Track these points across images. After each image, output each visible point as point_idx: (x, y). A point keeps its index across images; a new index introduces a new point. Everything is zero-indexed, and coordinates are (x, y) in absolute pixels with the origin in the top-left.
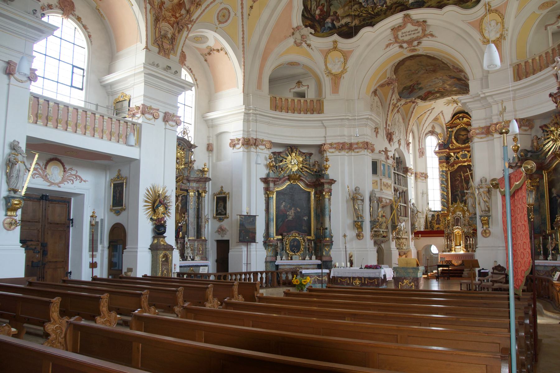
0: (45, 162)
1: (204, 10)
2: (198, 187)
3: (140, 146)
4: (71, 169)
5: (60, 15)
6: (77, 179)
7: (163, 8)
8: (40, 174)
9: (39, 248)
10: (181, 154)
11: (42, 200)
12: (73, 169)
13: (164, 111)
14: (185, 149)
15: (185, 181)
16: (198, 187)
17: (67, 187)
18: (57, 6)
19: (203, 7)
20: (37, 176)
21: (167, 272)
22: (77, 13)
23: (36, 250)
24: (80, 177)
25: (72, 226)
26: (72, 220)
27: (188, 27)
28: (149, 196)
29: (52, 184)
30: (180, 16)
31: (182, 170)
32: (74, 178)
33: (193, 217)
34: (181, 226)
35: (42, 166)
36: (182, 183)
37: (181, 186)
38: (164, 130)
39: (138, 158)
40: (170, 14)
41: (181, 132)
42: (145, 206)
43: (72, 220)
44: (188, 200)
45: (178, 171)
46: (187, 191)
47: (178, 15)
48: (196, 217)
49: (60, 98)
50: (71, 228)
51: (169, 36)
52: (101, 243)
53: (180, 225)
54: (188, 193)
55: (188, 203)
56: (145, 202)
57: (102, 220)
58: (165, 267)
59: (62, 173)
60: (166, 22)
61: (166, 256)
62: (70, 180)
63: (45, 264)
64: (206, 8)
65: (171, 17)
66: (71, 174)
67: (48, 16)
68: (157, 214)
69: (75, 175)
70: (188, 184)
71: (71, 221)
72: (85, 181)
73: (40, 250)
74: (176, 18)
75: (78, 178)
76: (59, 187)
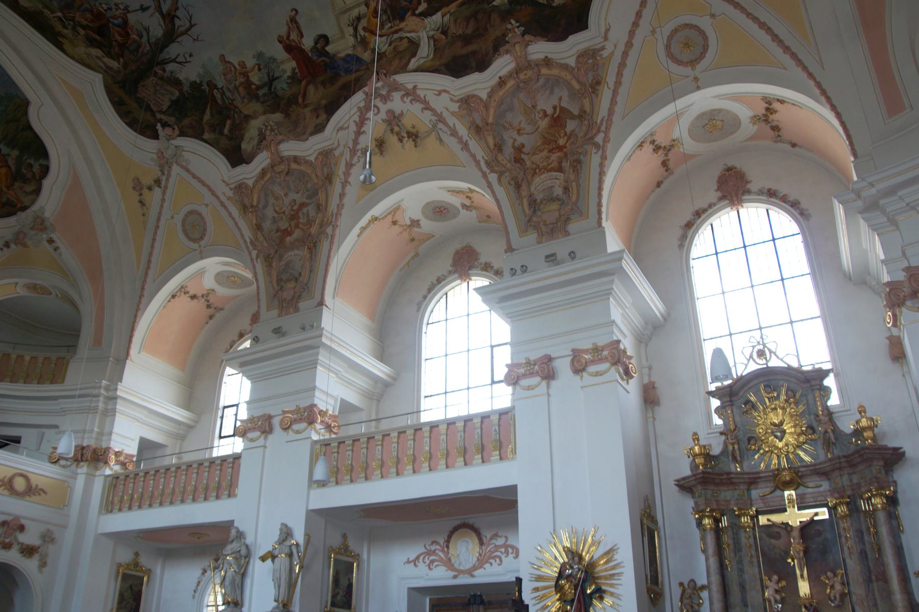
1: (618, 83)
4: (496, 536)
5: (459, 281)
7: (523, 156)
8: (441, 560)
11: (471, 606)
12: (500, 534)
18: (450, 273)
19: (611, 79)
20: (435, 564)
22: (483, 260)
24: (513, 547)
27: (597, 146)
29: (459, 572)
30: (569, 139)
32: (501, 552)
33: (861, 579)
35: (442, 544)
40: (545, 153)
41: (751, 357)
47: (561, 142)
49: (452, 414)
51: (558, 191)
60: (542, 174)
64: (620, 74)
65: (548, 158)
66: (496, 546)
67: (446, 294)
69: (501, 546)
74: (560, 148)
76: (473, 576)
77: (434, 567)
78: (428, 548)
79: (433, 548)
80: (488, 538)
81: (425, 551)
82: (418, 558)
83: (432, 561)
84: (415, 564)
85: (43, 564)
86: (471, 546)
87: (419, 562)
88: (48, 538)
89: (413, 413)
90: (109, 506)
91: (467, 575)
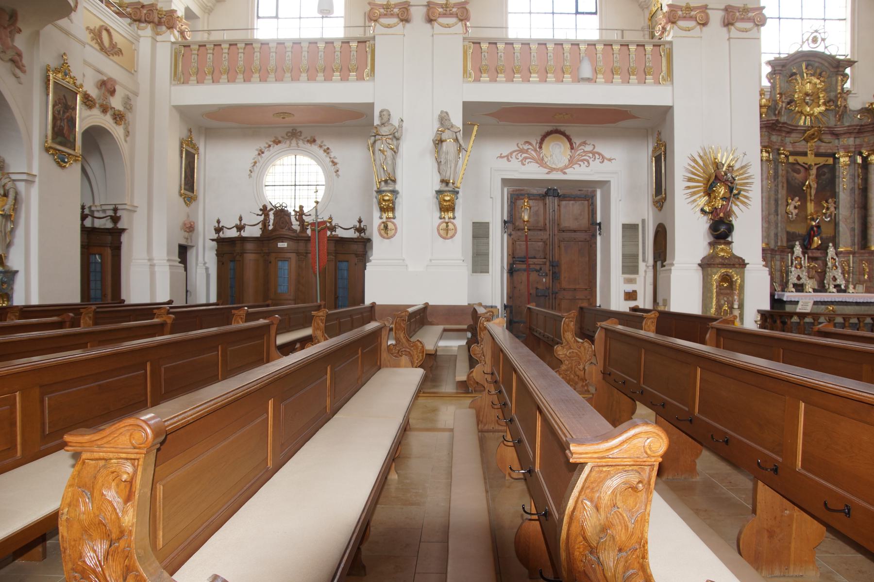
0: (539, 140)
2: (859, 145)
3: (672, 81)
4: (584, 143)
6: (595, 159)
8: (533, 158)
9: (547, 268)
10: (815, 84)
11: (547, 197)
12: (588, 142)
13: (723, 7)
14: (824, 73)
15: (827, 138)
16: (861, 146)
17: (579, 173)
20: (528, 160)
21: (729, 308)
23: (541, 272)
24: (599, 154)
25: (600, 234)
26: (600, 224)
28: (697, 170)
29: (552, 170)
31: (820, 117)
32: (589, 157)
34: (818, 227)
36: (821, 140)
37: (818, 147)
38: (728, 42)
39: (670, 104)
42: (688, 188)
43: (600, 224)
44: (837, 174)
45: (811, 120)
46: (833, 155)
48: (856, 206)
50: (599, 238)
52: (644, 260)
53: (814, 224)
54: (837, 161)
55: (837, 180)
56: (688, 181)
57: (643, 221)
58: (725, 299)
59: (568, 152)
61: (726, 278)
62: (582, 161)
63: (557, 293)
66: (584, 152)
68: (712, 202)
70: (837, 141)
71: (598, 227)
72: (610, 160)
73: (548, 272)
75: (597, 156)
76: (565, 173)
77: (526, 163)
78: (521, 147)
79: (526, 147)
80: (577, 145)
81: (518, 149)
82: (511, 153)
83: (526, 158)
84: (508, 160)
85: (127, 133)
86: (563, 148)
87: (511, 158)
88: (128, 103)
89: (503, 28)
90: (180, 76)
91: (559, 172)
